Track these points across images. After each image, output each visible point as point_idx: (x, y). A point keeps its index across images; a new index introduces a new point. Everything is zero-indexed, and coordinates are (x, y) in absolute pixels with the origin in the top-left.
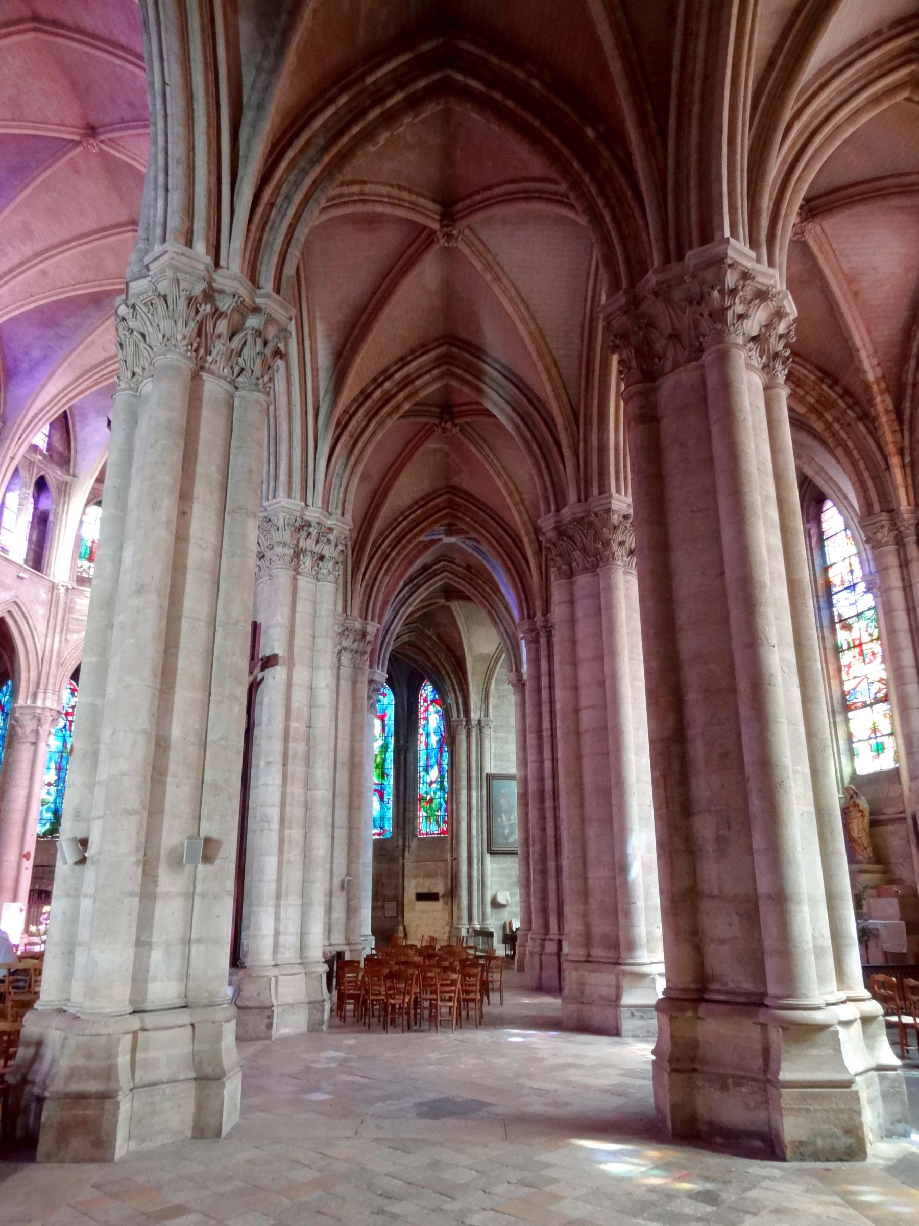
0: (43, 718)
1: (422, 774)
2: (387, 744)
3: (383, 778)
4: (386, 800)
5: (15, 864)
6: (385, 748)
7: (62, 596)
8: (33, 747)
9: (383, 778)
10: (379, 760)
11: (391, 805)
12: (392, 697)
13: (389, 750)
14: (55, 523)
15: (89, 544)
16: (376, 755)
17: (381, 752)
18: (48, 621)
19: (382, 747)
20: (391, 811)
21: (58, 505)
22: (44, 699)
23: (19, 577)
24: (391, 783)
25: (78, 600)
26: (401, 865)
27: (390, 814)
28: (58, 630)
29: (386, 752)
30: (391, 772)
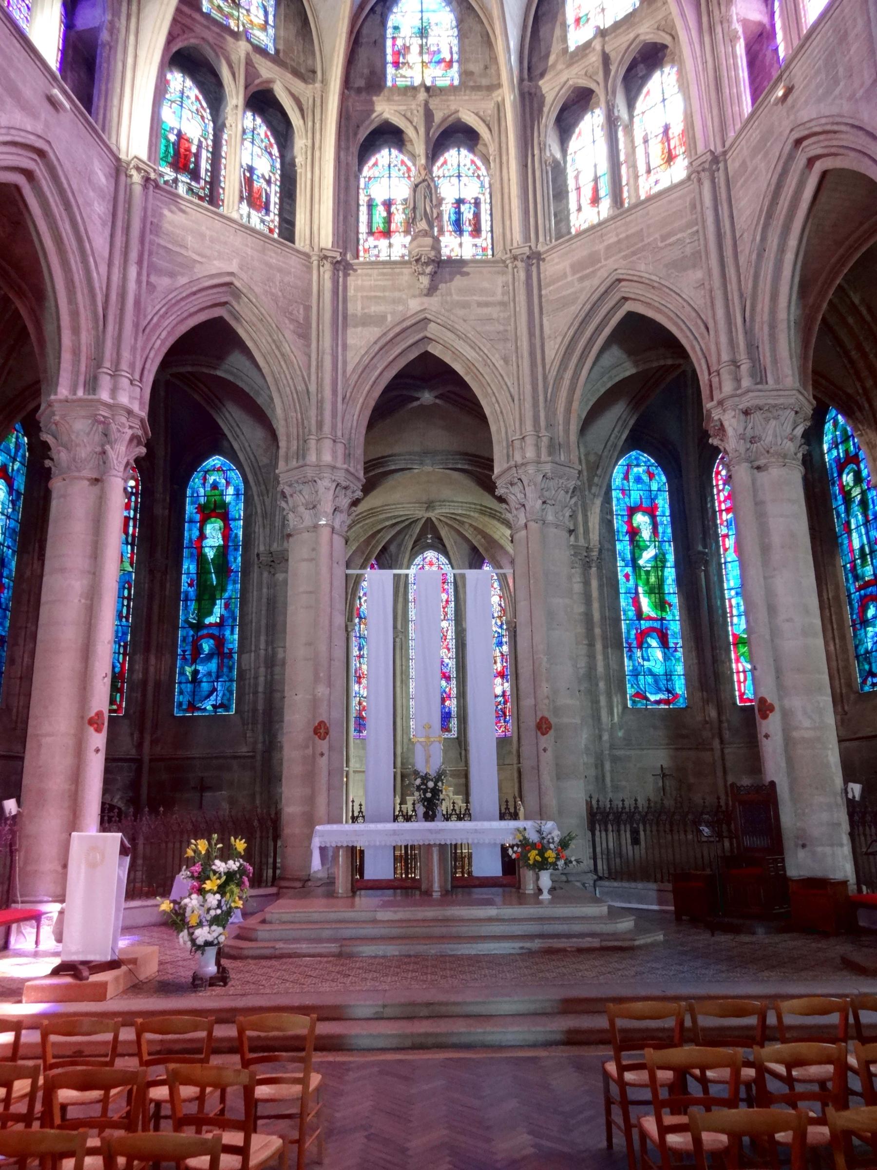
0: (113, 427)
1: (734, 602)
2: (664, 555)
3: (663, 609)
4: (671, 645)
5: (70, 742)
6: (660, 560)
7: (138, 189)
8: (96, 489)
9: (663, 609)
10: (653, 579)
11: (679, 654)
12: (664, 479)
13: (668, 564)
14: (112, 48)
15: (173, 138)
16: (648, 573)
17: (655, 567)
18: (112, 236)
19: (656, 557)
20: (681, 664)
21: (116, 13)
22: (114, 391)
23: (52, 102)
24: (677, 618)
25: (166, 212)
26: (718, 753)
27: (680, 669)
28: (134, 255)
29: (664, 567)
30: (674, 600)
